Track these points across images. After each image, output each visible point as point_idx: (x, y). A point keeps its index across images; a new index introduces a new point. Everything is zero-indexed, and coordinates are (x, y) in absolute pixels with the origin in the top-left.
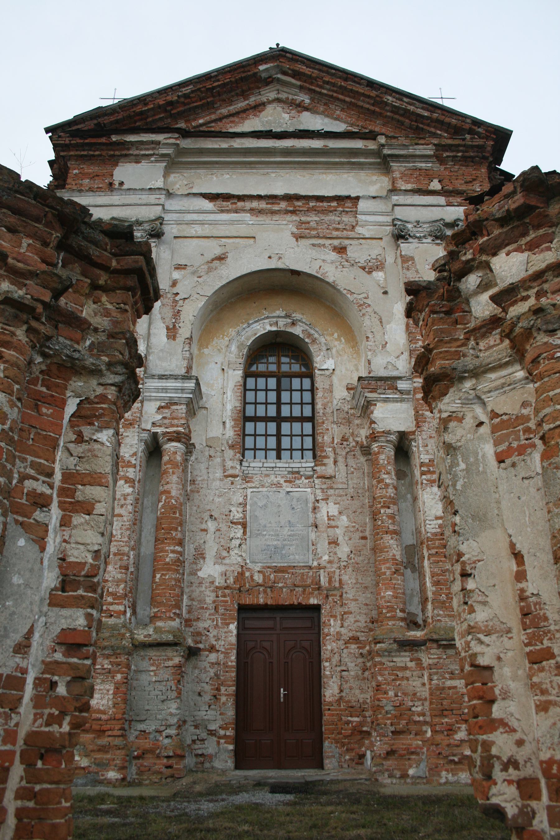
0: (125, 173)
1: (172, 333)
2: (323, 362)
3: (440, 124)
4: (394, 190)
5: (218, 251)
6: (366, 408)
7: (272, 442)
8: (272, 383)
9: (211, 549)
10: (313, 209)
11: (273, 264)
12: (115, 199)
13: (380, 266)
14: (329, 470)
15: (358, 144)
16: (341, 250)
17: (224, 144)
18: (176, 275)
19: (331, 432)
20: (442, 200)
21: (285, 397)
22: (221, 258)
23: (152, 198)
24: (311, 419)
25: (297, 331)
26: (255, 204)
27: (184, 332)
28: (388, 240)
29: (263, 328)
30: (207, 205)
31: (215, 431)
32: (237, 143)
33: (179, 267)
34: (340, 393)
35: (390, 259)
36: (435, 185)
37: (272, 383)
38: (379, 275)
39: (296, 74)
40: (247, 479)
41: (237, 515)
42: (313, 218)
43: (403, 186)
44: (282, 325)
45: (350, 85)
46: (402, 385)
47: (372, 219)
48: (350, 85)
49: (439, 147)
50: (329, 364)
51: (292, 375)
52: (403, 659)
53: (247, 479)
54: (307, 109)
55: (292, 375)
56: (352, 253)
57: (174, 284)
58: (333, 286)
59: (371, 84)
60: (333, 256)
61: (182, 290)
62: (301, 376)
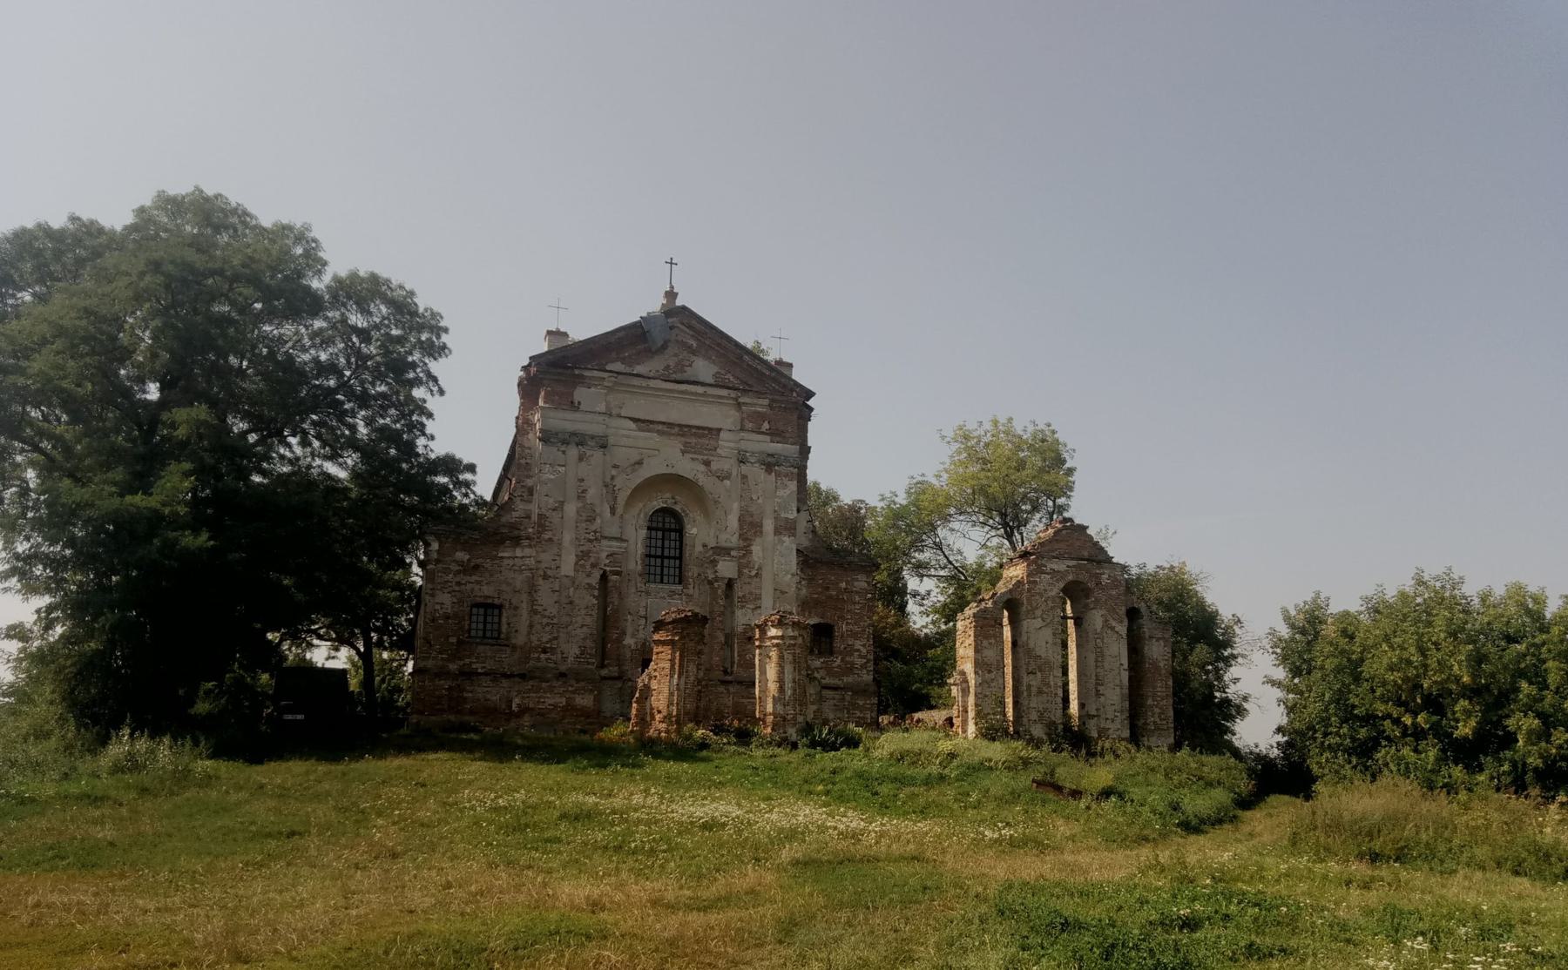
0: (580, 394)
1: (613, 511)
2: (691, 530)
3: (774, 380)
4: (742, 429)
5: (638, 458)
6: (714, 563)
7: (658, 570)
8: (660, 534)
9: (629, 631)
10: (695, 435)
11: (669, 471)
12: (577, 416)
13: (728, 477)
14: (691, 591)
15: (724, 392)
16: (707, 463)
17: (644, 383)
18: (614, 472)
19: (692, 571)
20: (768, 438)
21: (667, 543)
22: (640, 463)
23: (601, 418)
24: (680, 558)
25: (678, 508)
26: (660, 427)
27: (620, 510)
28: (733, 461)
29: (658, 504)
30: (632, 425)
31: (632, 566)
32: (652, 383)
33: (615, 466)
34: (699, 548)
35: (734, 473)
36: (766, 426)
37: (660, 534)
38: (727, 482)
39: (690, 327)
40: (648, 593)
41: (642, 613)
42: (694, 440)
43: (750, 425)
44: (670, 504)
45: (724, 342)
46: (733, 553)
47: (727, 443)
48: (724, 342)
49: (773, 401)
50: (694, 531)
51: (670, 530)
52: (722, 689)
53: (648, 593)
54: (694, 352)
55: (670, 530)
56: (714, 466)
57: (613, 478)
58: (701, 488)
59: (737, 344)
60: (702, 468)
61: (618, 483)
62: (675, 531)
